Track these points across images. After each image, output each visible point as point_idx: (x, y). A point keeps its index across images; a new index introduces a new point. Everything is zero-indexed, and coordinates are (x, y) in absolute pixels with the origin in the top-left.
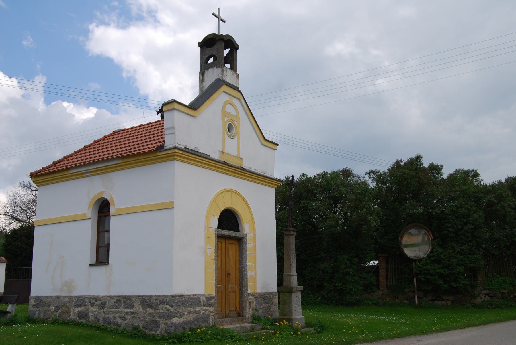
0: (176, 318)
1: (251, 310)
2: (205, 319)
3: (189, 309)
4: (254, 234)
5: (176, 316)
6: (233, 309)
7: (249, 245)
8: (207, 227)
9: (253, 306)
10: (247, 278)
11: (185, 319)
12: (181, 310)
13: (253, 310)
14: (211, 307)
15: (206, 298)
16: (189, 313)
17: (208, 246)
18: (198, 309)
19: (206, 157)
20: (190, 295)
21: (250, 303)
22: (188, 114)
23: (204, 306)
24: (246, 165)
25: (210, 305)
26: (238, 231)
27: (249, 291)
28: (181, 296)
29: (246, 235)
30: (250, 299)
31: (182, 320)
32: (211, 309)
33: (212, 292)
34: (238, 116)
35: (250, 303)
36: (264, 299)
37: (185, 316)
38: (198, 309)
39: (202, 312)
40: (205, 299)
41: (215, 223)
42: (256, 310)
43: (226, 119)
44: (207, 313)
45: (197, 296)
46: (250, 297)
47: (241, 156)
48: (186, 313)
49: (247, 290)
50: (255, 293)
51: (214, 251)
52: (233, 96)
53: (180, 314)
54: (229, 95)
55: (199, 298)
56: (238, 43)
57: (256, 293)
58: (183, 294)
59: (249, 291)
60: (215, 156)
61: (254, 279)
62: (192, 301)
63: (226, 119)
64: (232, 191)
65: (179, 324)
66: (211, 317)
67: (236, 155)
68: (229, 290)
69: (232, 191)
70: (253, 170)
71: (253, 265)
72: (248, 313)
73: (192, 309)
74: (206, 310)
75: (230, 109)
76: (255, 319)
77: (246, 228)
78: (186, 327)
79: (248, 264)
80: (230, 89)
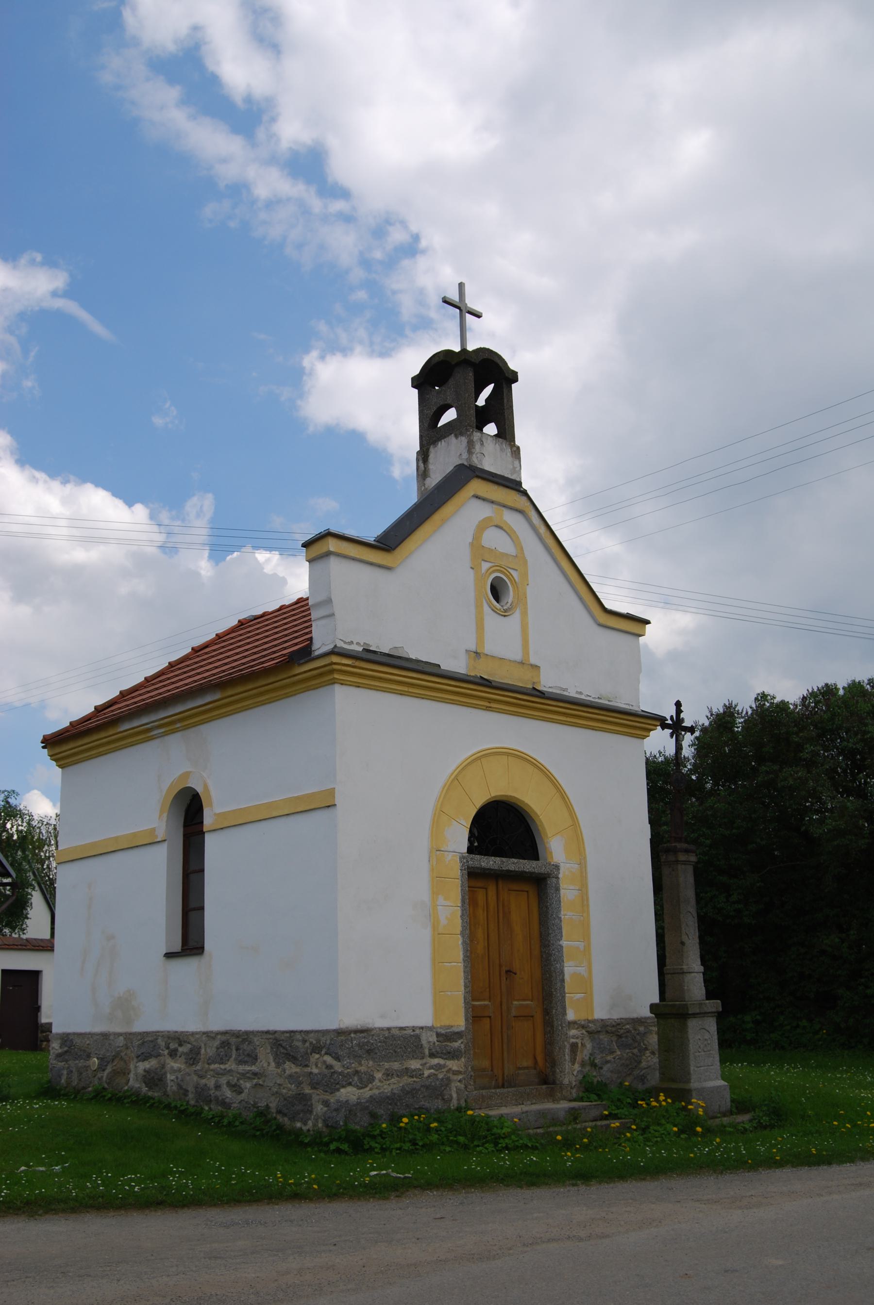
0: (349, 1089)
1: (577, 1067)
2: (438, 1090)
3: (387, 1065)
4: (582, 864)
5: (350, 1084)
6: (525, 1064)
7: (567, 892)
8: (436, 851)
9: (584, 1054)
10: (563, 981)
11: (376, 1092)
12: (362, 1069)
13: (583, 1064)
14: (453, 1058)
15: (438, 1035)
16: (388, 1074)
17: (441, 900)
18: (414, 1064)
19: (430, 670)
20: (389, 1029)
22: (371, 564)
23: (432, 1055)
24: (548, 682)
25: (453, 1055)
26: (536, 857)
27: (571, 1016)
28: (362, 1031)
29: (557, 867)
30: (573, 1037)
31: (366, 1093)
32: (453, 1065)
33: (458, 1021)
34: (520, 557)
35: (574, 1046)
36: (620, 1037)
37: (376, 1083)
38: (414, 1064)
39: (427, 1073)
40: (434, 1039)
41: (458, 838)
42: (593, 1065)
43: (485, 566)
44: (441, 1076)
45: (410, 1032)
46: (573, 1032)
47: (533, 660)
48: (378, 1075)
49: (564, 1013)
50: (589, 1021)
51: (459, 913)
52: (504, 506)
53: (360, 1080)
54: (492, 502)
55: (418, 1037)
56: (512, 366)
57: (594, 1021)
58: (370, 1026)
59: (571, 1016)
60: (457, 664)
62: (400, 1043)
63: (485, 566)
64: (508, 754)
65: (358, 1104)
66: (454, 1086)
67: (518, 657)
68: (514, 1013)
69: (508, 754)
70: (572, 693)
71: (581, 945)
72: (570, 1073)
73: (396, 1066)
74: (439, 1067)
75: (494, 539)
76: (591, 1089)
77: (556, 849)
78: (381, 1112)
79: (564, 943)
80: (495, 487)
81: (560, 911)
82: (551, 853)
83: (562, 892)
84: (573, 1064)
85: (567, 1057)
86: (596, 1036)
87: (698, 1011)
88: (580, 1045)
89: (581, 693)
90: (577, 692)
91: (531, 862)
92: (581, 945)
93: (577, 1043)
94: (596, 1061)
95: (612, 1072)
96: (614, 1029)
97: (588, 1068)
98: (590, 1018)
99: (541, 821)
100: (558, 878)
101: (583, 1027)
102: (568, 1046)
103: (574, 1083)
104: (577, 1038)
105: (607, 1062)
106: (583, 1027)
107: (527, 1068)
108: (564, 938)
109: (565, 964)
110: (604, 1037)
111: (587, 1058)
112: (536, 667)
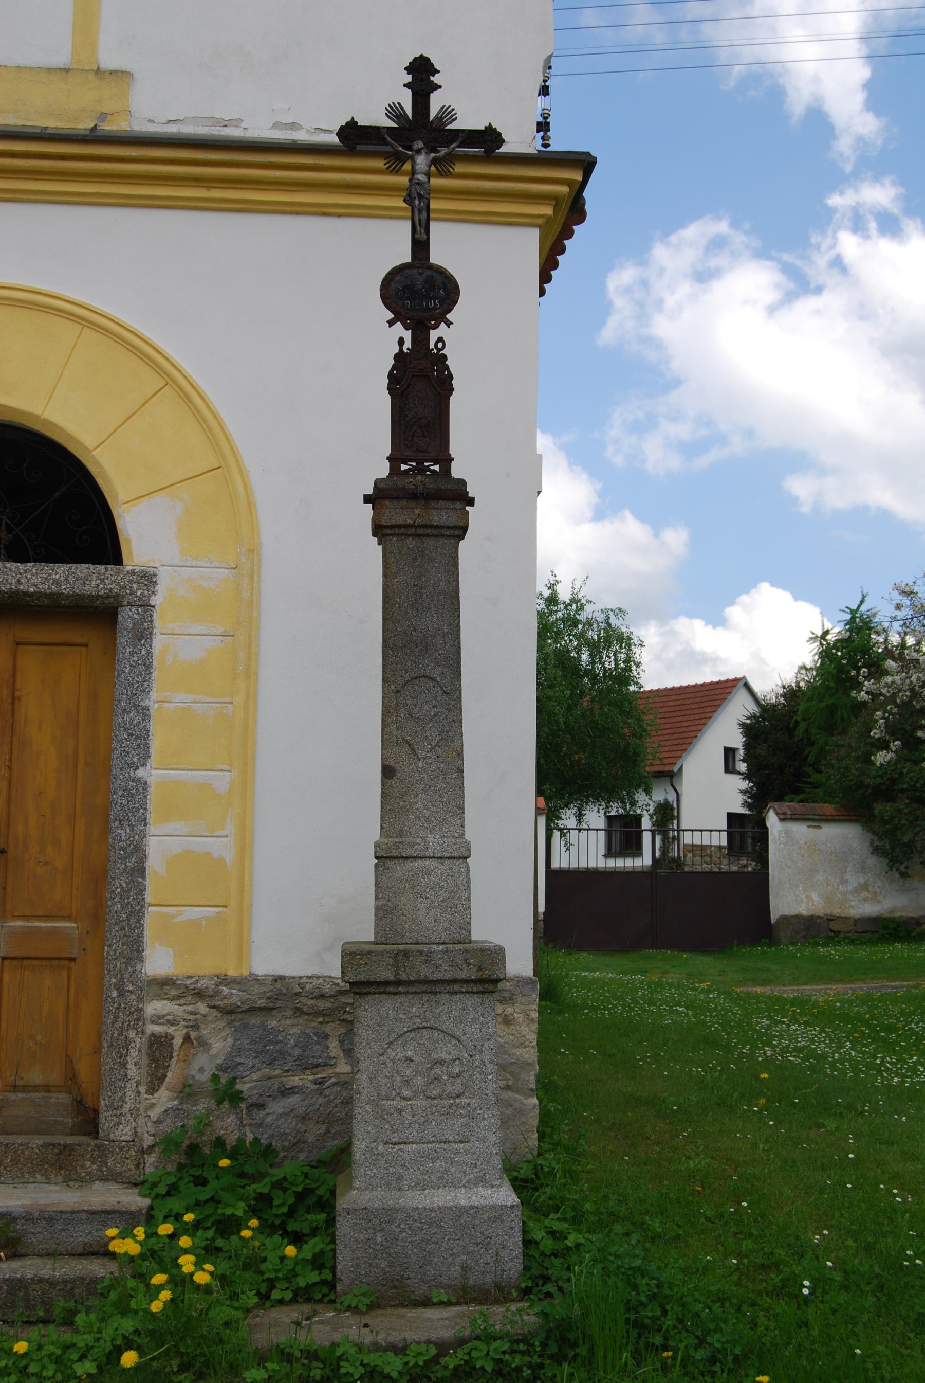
1: (164, 1098)
4: (247, 565)
6: (36, 1076)
7: (178, 642)
9: (203, 1066)
10: (140, 870)
21: (159, 1048)
24: (153, 107)
26: (117, 559)
27: (158, 961)
29: (148, 579)
30: (157, 1019)
35: (159, 1048)
42: (229, 1095)
46: (153, 1007)
47: (109, 60)
50: (224, 980)
59: (158, 961)
61: (229, 889)
67: (61, 57)
70: (259, 128)
72: (142, 1112)
76: (191, 1160)
77: (146, 531)
79: (153, 774)
81: (146, 692)
82: (129, 541)
83: (159, 643)
84: (152, 1090)
85: (132, 1070)
86: (254, 1020)
87: (389, 975)
88: (178, 1041)
89: (293, 126)
90: (276, 126)
91: (47, 568)
92: (222, 782)
93: (169, 1038)
94: (243, 1087)
95: (304, 1118)
96: (322, 1005)
97: (203, 1106)
98: (232, 973)
99: (97, 463)
100: (147, 607)
101: (200, 994)
102: (138, 1042)
103: (148, 1141)
104: (172, 1023)
105: (285, 1092)
106: (200, 994)
107: (47, 1088)
108: (153, 761)
109: (152, 829)
110: (291, 1029)
111: (205, 1077)
112: (121, 76)
